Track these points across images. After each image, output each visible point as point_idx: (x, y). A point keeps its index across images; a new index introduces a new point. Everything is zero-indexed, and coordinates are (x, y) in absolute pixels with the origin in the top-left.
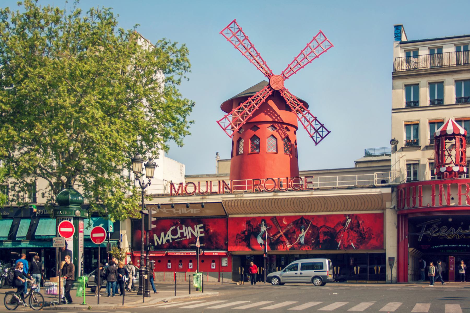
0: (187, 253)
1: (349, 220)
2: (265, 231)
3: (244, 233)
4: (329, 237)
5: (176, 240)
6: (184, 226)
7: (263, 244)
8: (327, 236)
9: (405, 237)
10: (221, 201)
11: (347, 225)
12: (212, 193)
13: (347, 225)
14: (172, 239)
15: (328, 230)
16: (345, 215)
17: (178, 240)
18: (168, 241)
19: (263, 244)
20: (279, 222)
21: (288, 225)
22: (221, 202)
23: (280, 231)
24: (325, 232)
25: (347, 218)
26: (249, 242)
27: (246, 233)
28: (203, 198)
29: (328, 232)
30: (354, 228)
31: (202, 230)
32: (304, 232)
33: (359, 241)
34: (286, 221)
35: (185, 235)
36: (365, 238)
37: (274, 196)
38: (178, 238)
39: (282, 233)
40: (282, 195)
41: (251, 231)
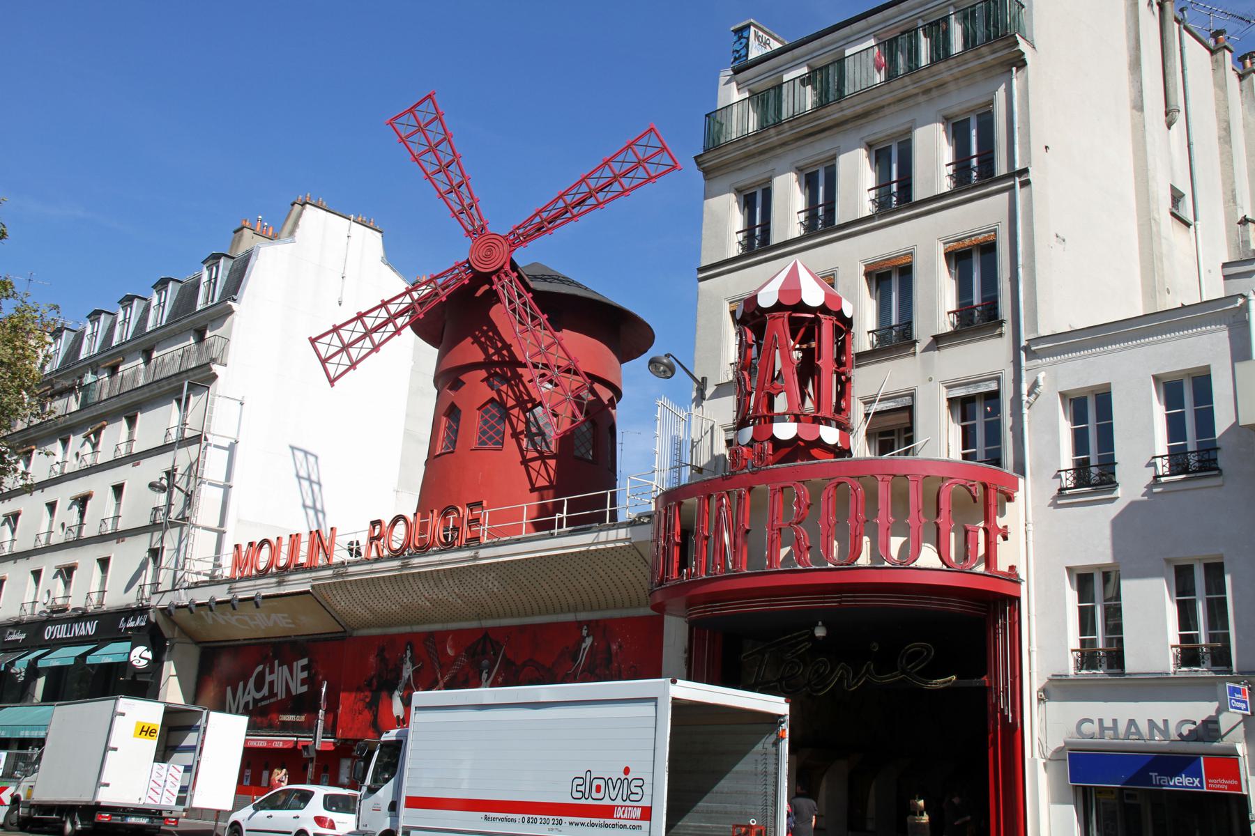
0: (268, 741)
1: (587, 638)
2: (409, 676)
5: (259, 705)
6: (276, 662)
7: (401, 717)
10: (307, 588)
11: (582, 658)
12: (300, 568)
14: (254, 698)
16: (579, 624)
17: (264, 703)
18: (247, 704)
19: (401, 717)
21: (455, 659)
22: (308, 592)
23: (439, 676)
25: (585, 632)
26: (378, 709)
27: (374, 681)
28: (280, 584)
31: (305, 674)
32: (486, 681)
34: (452, 647)
35: (275, 691)
38: (264, 698)
40: (420, 563)
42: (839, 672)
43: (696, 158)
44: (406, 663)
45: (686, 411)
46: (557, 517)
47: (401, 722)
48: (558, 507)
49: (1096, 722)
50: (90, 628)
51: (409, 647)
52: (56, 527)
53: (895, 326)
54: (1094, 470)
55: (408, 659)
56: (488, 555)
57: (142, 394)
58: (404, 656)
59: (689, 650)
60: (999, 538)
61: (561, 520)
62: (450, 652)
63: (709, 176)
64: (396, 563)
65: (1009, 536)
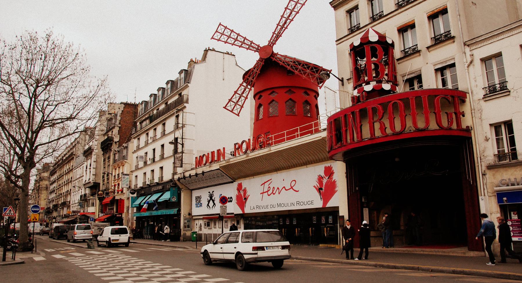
9: (355, 189)
10: (219, 168)
37: (247, 157)
43: (330, 3)
46: (296, 134)
48: (296, 131)
49: (507, 180)
50: (160, 187)
52: (148, 159)
53: (411, 47)
54: (498, 86)
56: (274, 148)
57: (168, 115)
59: (347, 173)
60: (461, 116)
63: (336, 9)
64: (245, 156)
65: (465, 116)
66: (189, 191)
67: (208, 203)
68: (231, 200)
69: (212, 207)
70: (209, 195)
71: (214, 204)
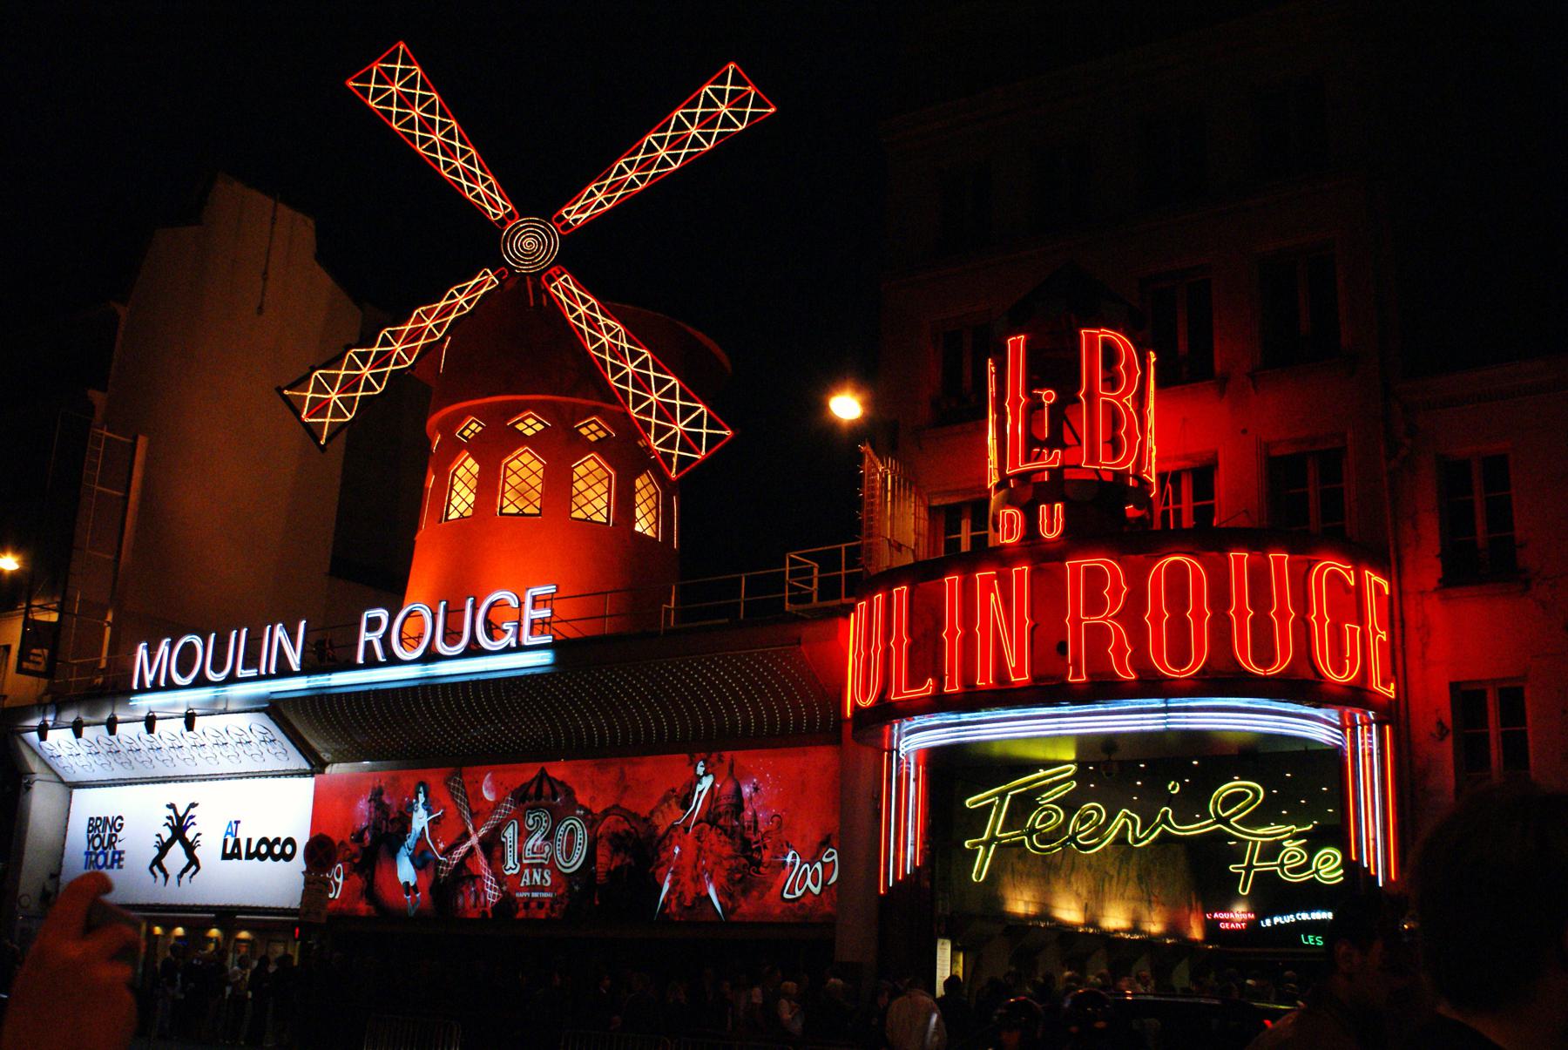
2: (423, 828)
3: (359, 836)
4: (628, 860)
8: (622, 855)
13: (697, 804)
15: (626, 826)
20: (470, 792)
21: (497, 804)
23: (471, 828)
24: (616, 835)
29: (628, 834)
30: (720, 815)
33: (738, 876)
36: (759, 863)
39: (474, 840)
41: (380, 829)
42: (1119, 821)
44: (416, 811)
45: (883, 465)
47: (411, 890)
51: (421, 789)
55: (420, 805)
58: (414, 801)
61: (668, 611)
62: (489, 796)
66: (58, 789)
67: (156, 852)
68: (289, 849)
69: (181, 876)
70: (170, 818)
71: (193, 861)
